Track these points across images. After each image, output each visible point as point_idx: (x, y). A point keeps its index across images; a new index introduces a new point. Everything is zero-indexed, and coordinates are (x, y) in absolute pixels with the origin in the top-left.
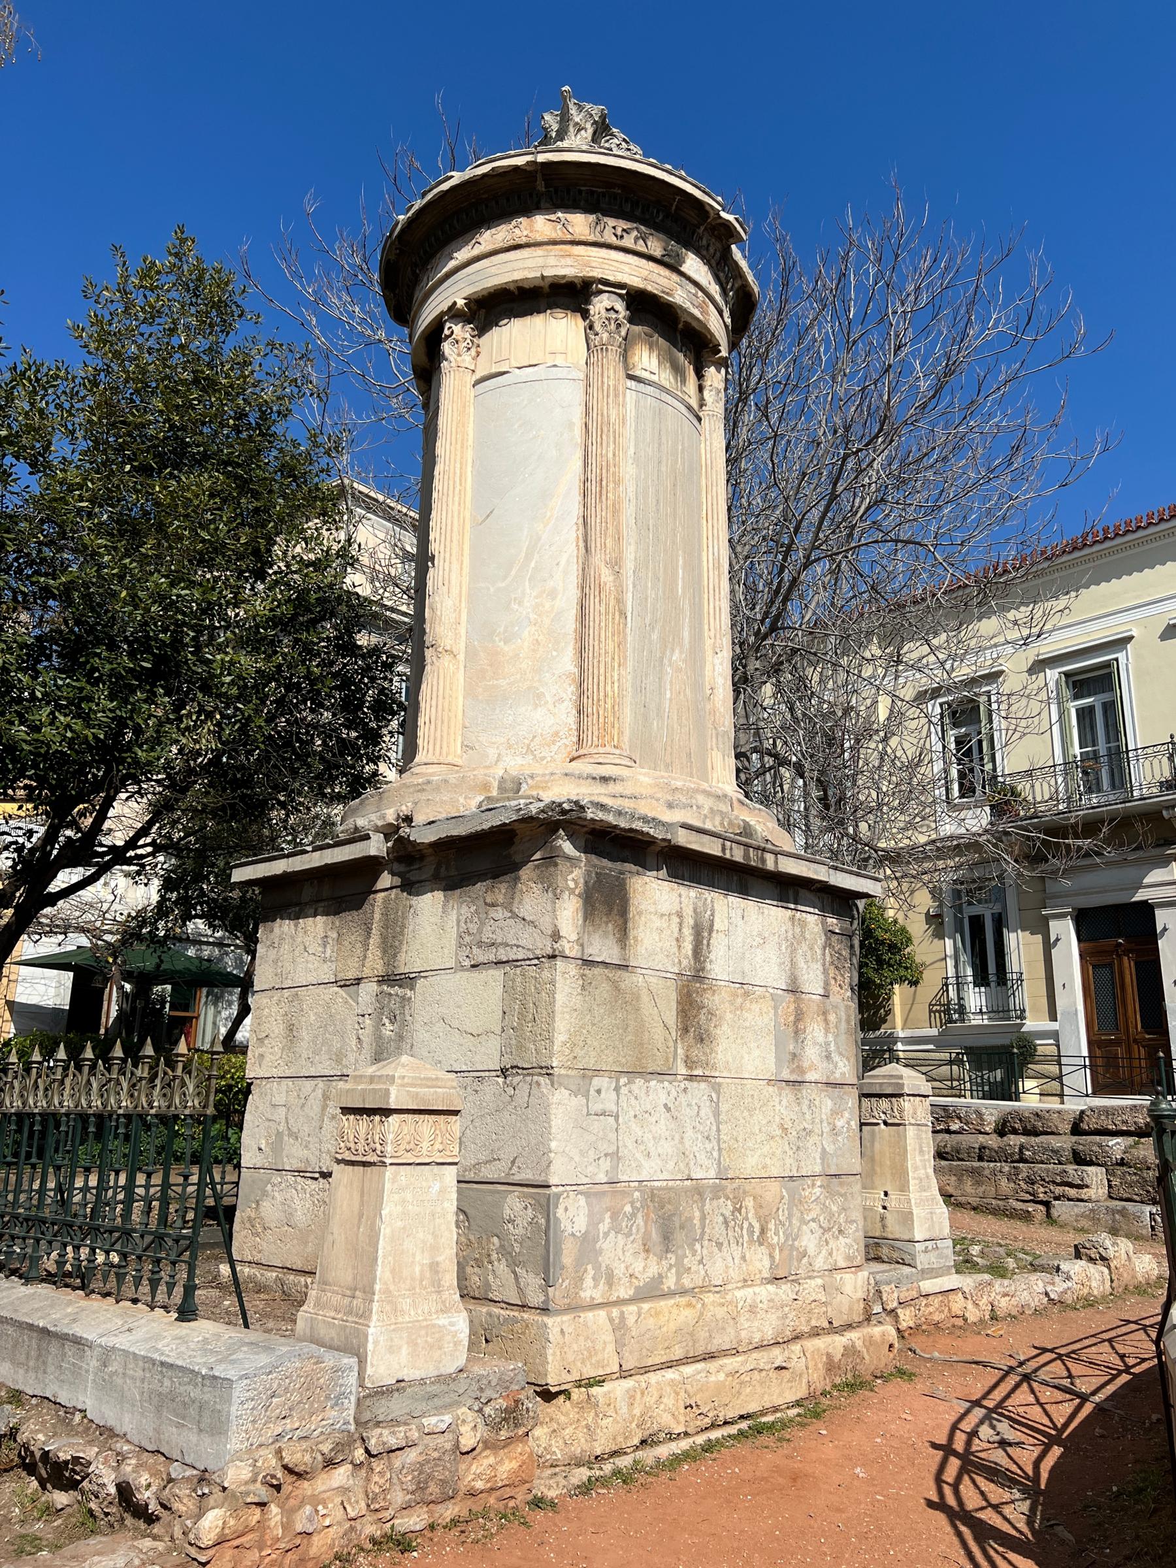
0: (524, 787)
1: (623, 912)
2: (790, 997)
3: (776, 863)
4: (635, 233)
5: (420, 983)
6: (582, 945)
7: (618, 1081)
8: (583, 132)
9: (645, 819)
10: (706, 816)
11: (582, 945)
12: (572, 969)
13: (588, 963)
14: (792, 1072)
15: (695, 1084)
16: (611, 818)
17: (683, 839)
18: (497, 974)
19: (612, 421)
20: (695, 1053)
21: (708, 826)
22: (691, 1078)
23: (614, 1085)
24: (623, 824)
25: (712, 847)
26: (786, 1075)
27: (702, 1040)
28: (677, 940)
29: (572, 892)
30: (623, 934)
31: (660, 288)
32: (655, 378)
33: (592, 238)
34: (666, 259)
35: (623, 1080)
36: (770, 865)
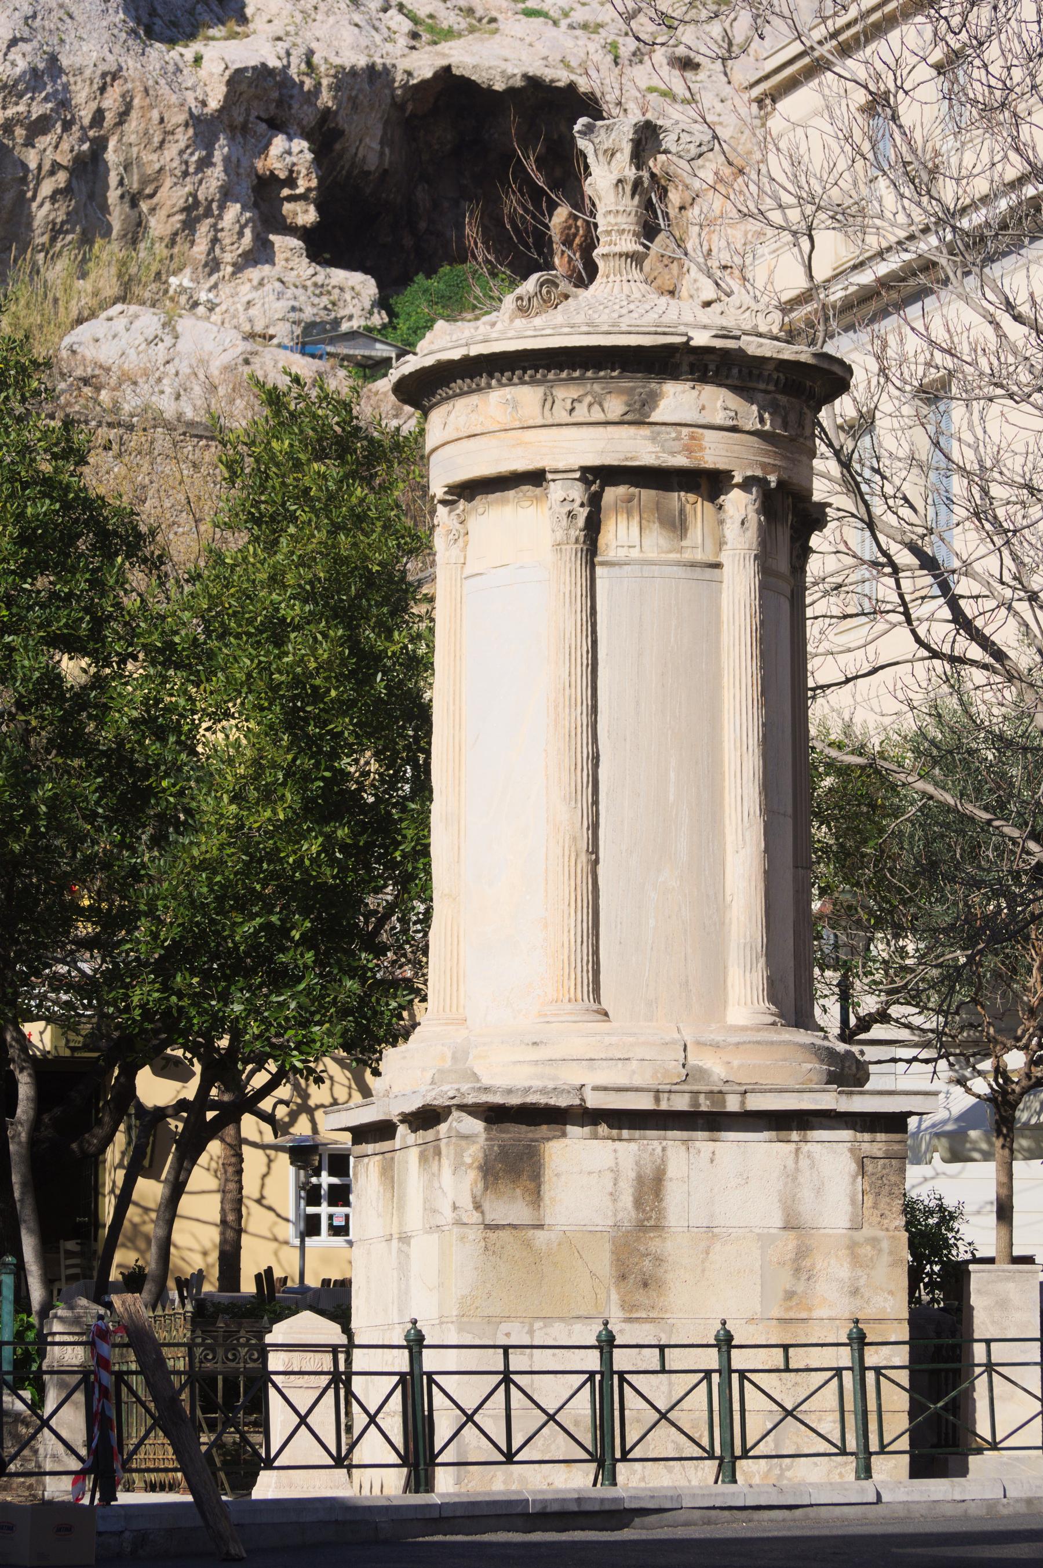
0: (471, 1057)
1: (536, 1177)
2: (791, 1235)
3: (743, 1103)
4: (589, 399)
5: (413, 1241)
6: (482, 1213)
7: (531, 1325)
8: (618, 155)
9: (543, 1091)
10: (634, 1072)
11: (482, 1213)
12: (475, 1234)
13: (488, 1227)
14: (788, 1309)
15: (636, 1326)
16: (498, 1099)
17: (594, 1101)
18: (436, 1236)
19: (567, 635)
20: (640, 1296)
21: (637, 1081)
22: (629, 1320)
23: (526, 1329)
24: (515, 1100)
25: (644, 1103)
26: (776, 1312)
27: (645, 1285)
28: (611, 1194)
29: (470, 1166)
30: (536, 1196)
31: (622, 457)
32: (635, 553)
33: (540, 421)
34: (627, 418)
35: (538, 1325)
36: (733, 1104)
